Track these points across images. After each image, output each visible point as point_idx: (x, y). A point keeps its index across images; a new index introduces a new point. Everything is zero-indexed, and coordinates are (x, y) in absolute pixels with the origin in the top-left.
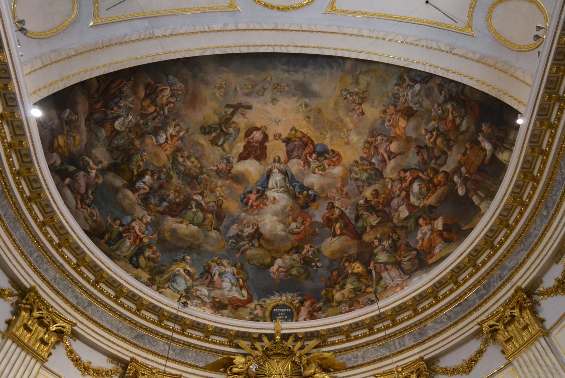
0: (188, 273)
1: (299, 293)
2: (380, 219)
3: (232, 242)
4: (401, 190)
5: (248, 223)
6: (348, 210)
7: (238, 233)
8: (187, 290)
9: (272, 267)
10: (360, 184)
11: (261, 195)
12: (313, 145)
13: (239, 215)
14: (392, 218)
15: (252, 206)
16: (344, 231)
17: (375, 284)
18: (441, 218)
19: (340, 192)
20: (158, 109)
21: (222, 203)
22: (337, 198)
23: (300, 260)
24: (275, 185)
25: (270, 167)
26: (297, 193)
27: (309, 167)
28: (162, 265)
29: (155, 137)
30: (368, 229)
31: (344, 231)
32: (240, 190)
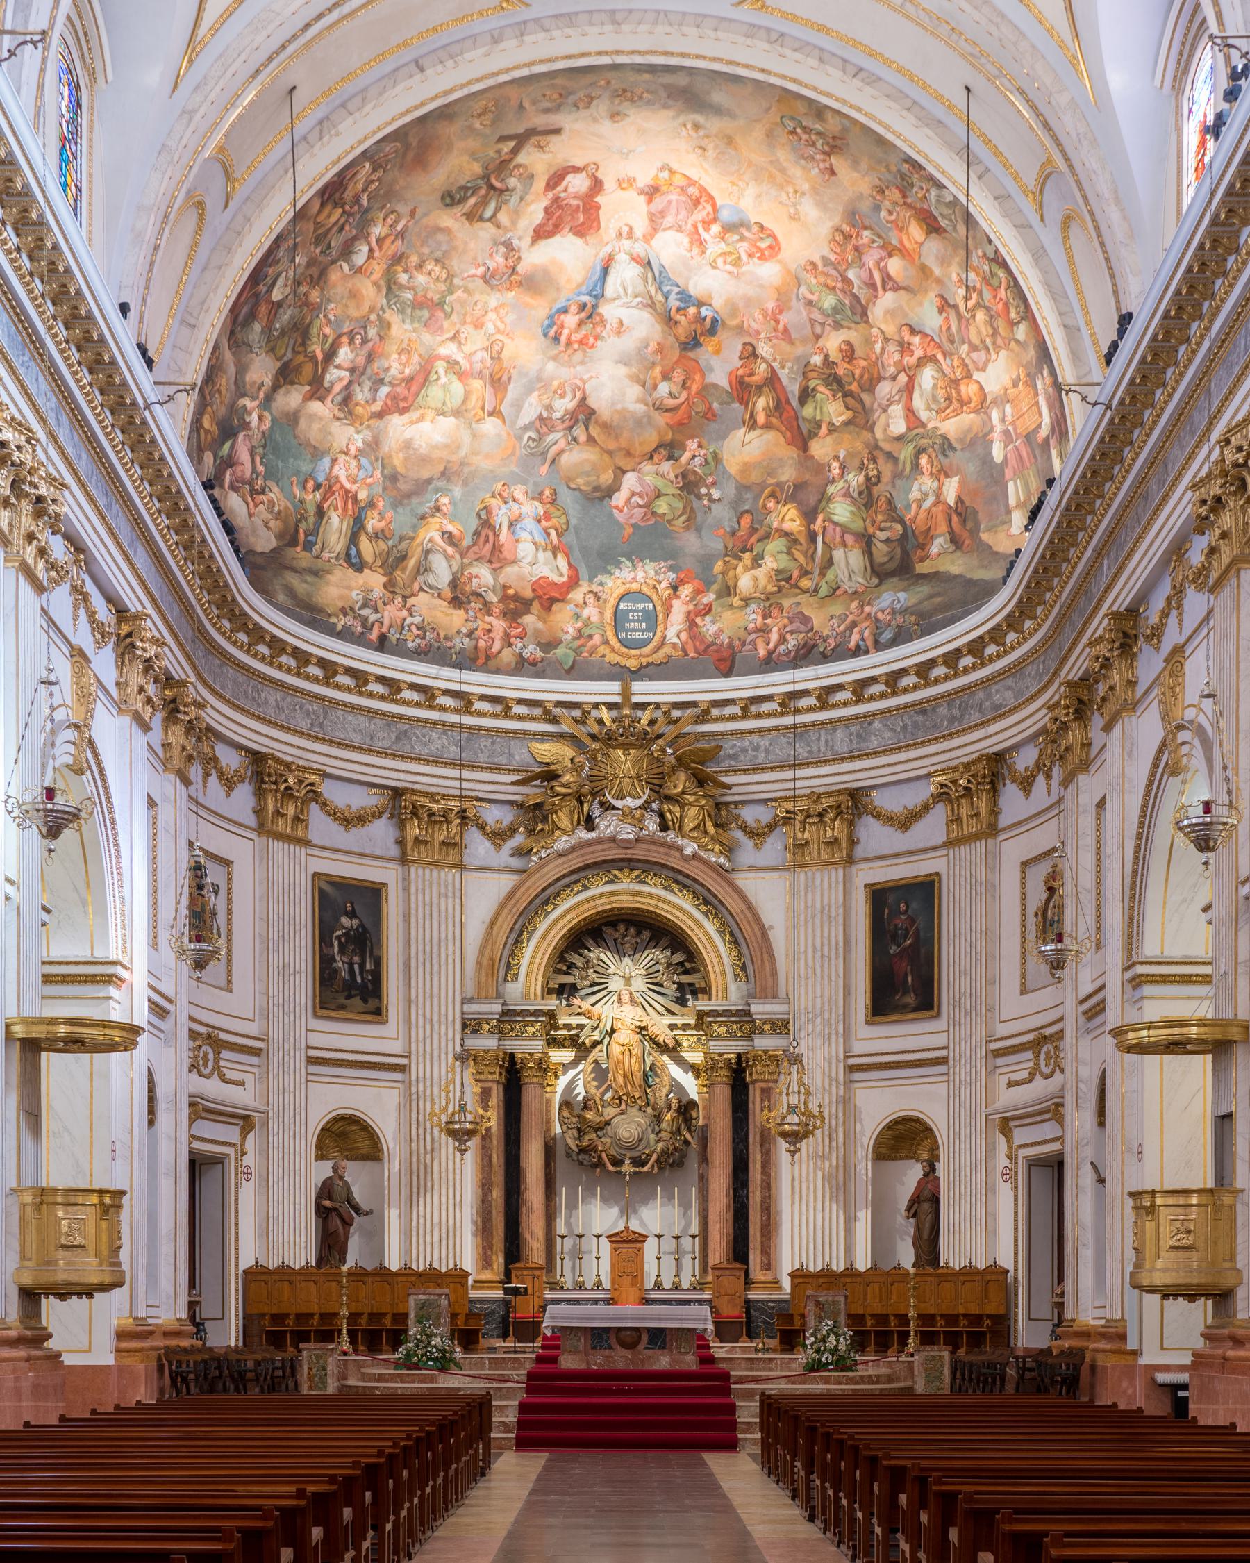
0: (449, 538)
1: (670, 562)
2: (849, 414)
3: (530, 438)
4: (901, 369)
5: (562, 386)
6: (787, 371)
7: (541, 415)
8: (454, 584)
9: (616, 495)
10: (817, 316)
11: (590, 316)
12: (714, 205)
13: (541, 370)
14: (874, 423)
15: (569, 343)
16: (774, 421)
17: (817, 570)
18: (956, 479)
19: (773, 322)
20: (347, 208)
21: (502, 347)
22: (763, 335)
23: (676, 477)
24: (622, 291)
25: (608, 249)
26: (674, 310)
27: (703, 252)
28: (401, 539)
29: (345, 261)
30: (824, 429)
31: (774, 421)
32: (540, 310)
